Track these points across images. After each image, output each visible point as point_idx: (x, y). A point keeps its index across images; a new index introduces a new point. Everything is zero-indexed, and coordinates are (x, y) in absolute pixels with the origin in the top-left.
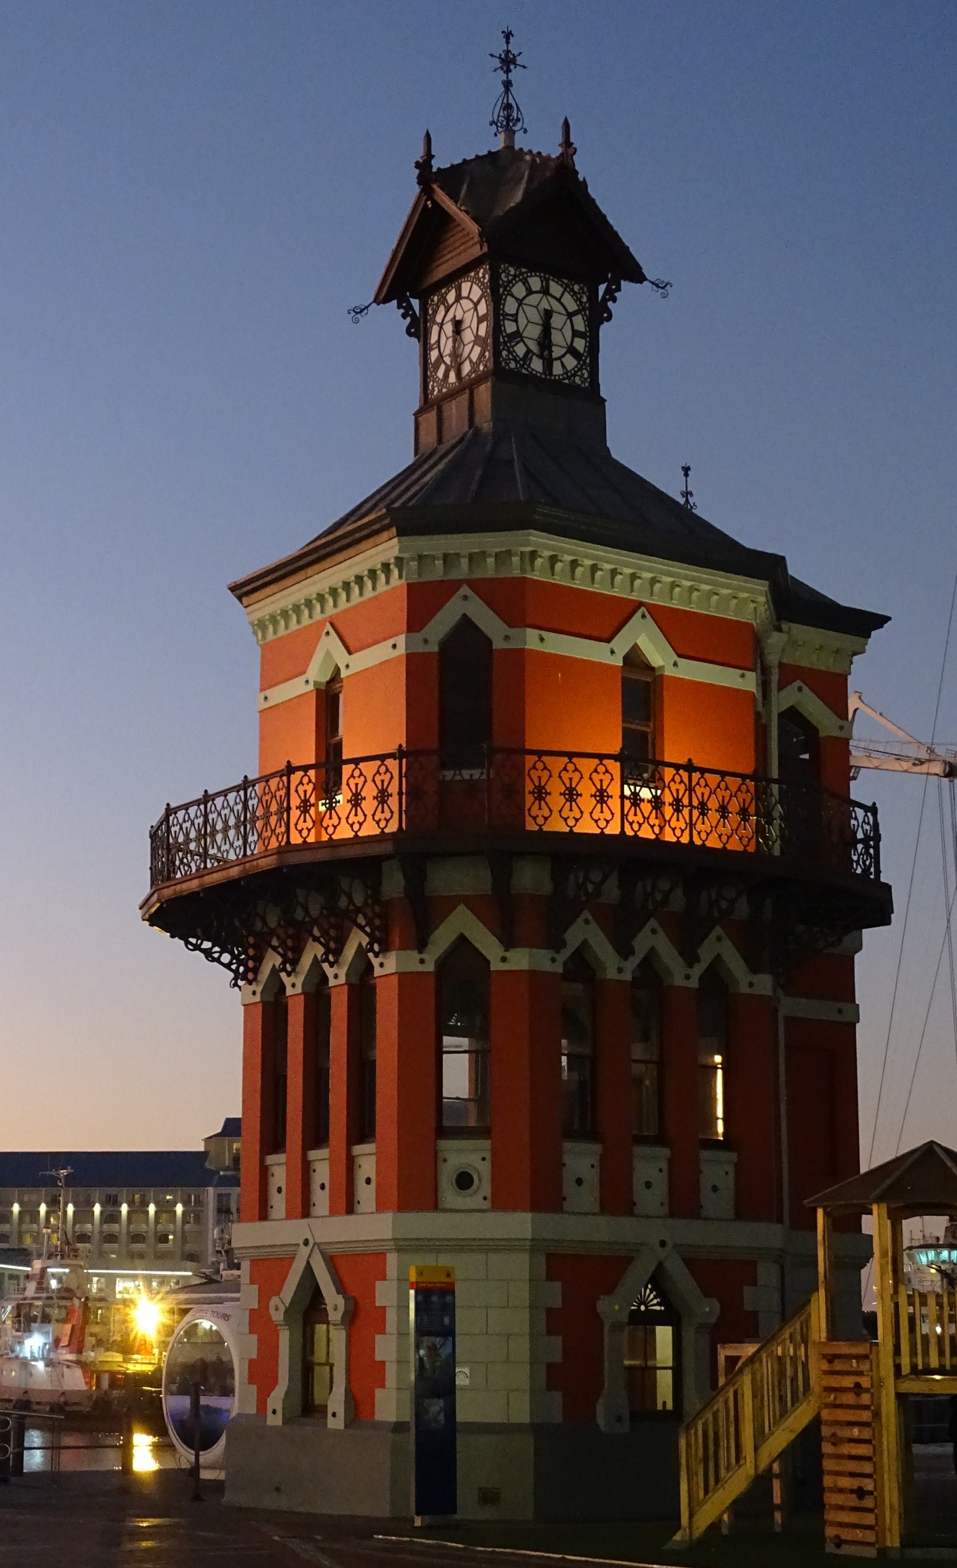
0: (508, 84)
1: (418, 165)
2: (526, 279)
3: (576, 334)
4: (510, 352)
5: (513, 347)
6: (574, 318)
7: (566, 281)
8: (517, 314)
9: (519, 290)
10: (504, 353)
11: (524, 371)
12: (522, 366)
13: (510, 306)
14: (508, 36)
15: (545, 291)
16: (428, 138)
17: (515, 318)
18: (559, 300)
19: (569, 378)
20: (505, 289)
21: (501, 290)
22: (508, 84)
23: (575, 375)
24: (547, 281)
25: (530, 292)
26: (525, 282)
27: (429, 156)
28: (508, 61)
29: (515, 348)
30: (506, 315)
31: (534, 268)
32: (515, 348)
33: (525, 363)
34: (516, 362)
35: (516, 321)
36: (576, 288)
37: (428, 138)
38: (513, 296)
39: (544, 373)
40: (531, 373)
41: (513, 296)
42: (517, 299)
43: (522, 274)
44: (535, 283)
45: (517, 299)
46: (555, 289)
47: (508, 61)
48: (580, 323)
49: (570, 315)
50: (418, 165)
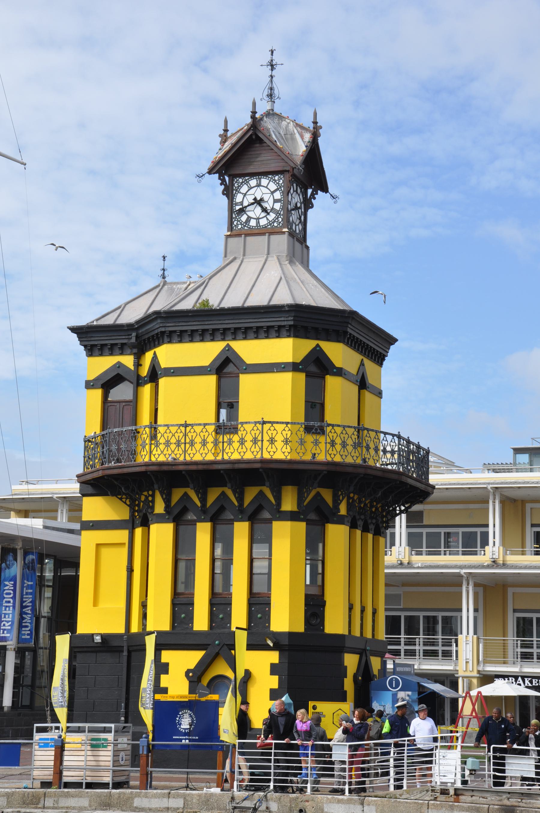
0: (272, 77)
1: (220, 136)
2: (248, 182)
3: (275, 201)
4: (238, 221)
5: (240, 218)
6: (274, 194)
7: (270, 176)
8: (242, 202)
9: (244, 189)
10: (235, 223)
11: (246, 228)
12: (245, 226)
13: (239, 198)
14: (272, 52)
15: (259, 185)
16: (226, 122)
17: (242, 203)
18: (266, 187)
19: (270, 225)
20: (236, 191)
21: (234, 192)
22: (272, 77)
23: (273, 223)
24: (260, 179)
25: (252, 188)
26: (247, 183)
27: (226, 130)
28: (272, 66)
29: (241, 219)
30: (237, 204)
31: (252, 175)
32: (241, 219)
33: (246, 224)
34: (241, 224)
35: (242, 205)
36: (277, 178)
37: (226, 122)
38: (241, 193)
39: (257, 225)
40: (250, 228)
41: (241, 193)
42: (242, 194)
43: (246, 180)
44: (253, 182)
45: (242, 194)
46: (264, 182)
47: (272, 66)
48: (278, 195)
49: (272, 193)
50: (220, 136)
